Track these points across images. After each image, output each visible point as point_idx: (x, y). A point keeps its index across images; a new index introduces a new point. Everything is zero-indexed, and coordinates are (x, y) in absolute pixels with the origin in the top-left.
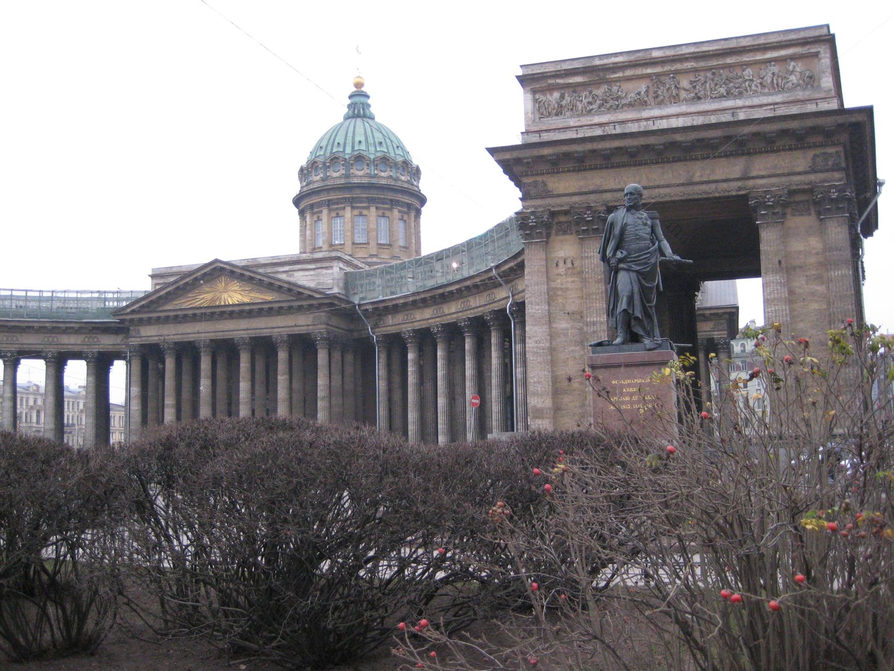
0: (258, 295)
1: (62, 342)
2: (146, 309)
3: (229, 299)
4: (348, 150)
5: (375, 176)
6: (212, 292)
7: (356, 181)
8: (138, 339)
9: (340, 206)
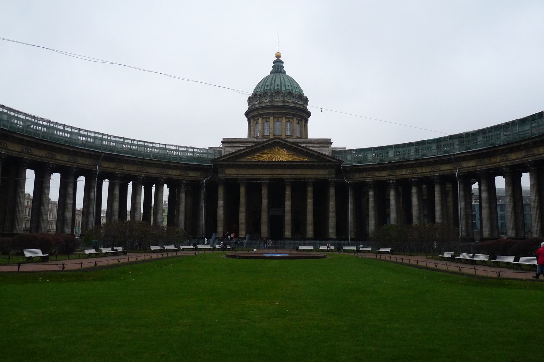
0: (297, 158)
1: (169, 173)
3: (280, 158)
4: (283, 89)
5: (296, 103)
6: (271, 154)
7: (288, 104)
8: (224, 175)
9: (279, 116)
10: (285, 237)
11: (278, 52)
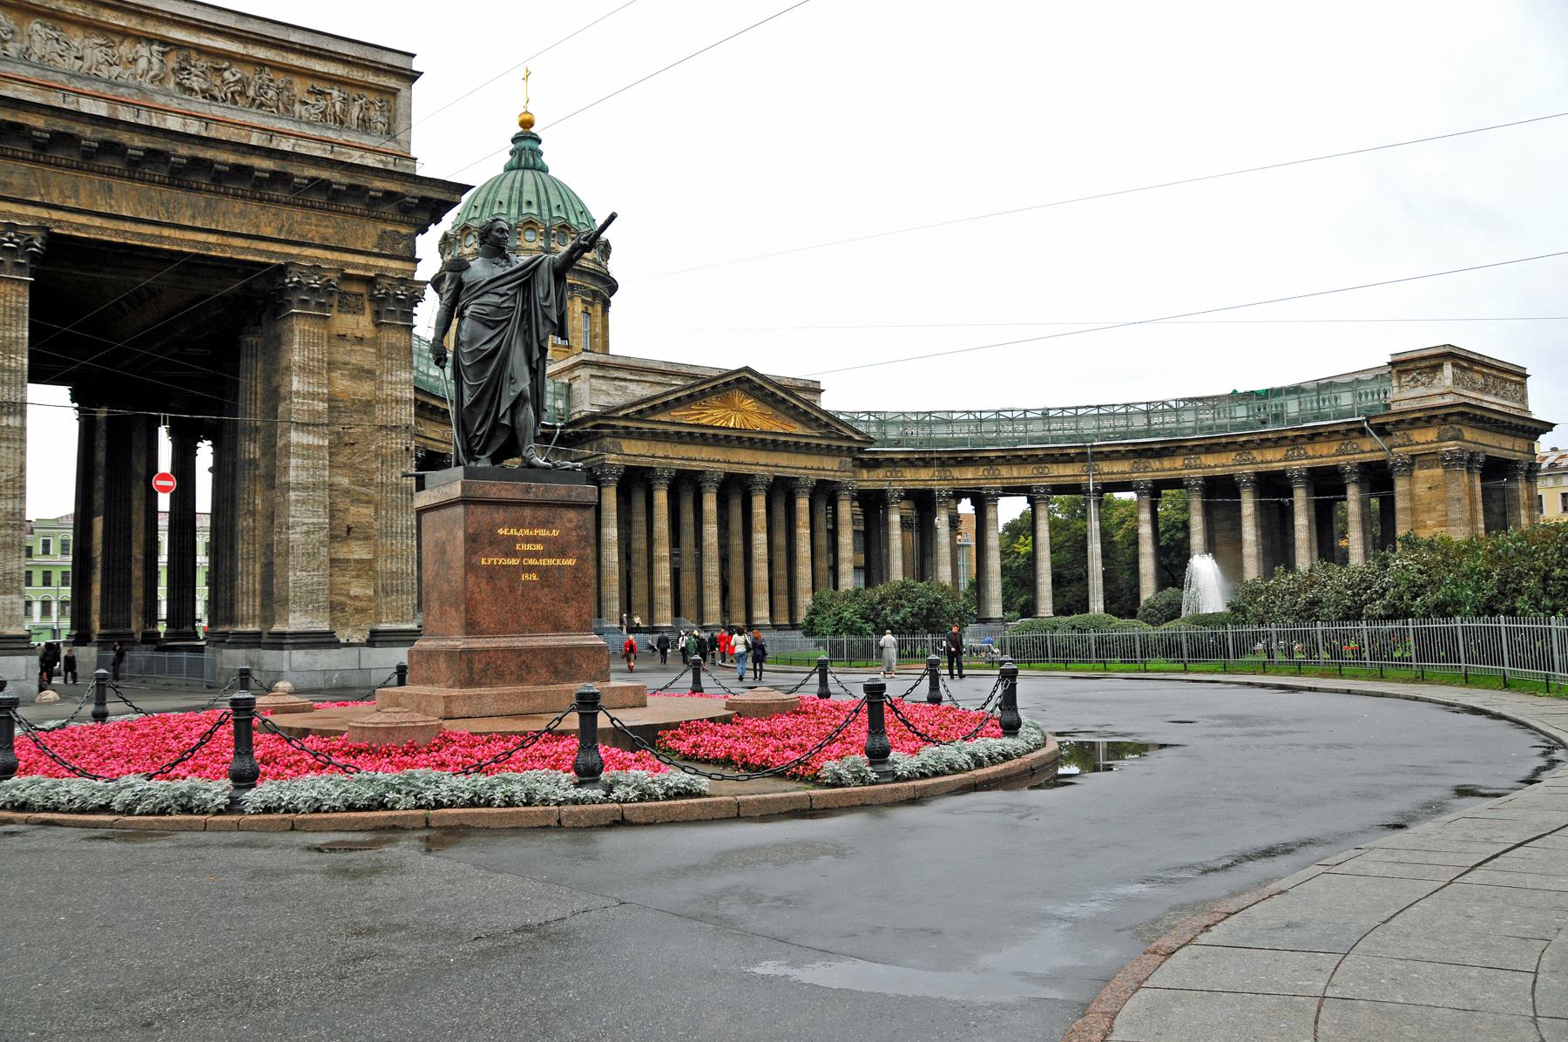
2: (638, 416)
4: (573, 221)
5: (600, 265)
8: (620, 457)
10: (758, 622)
11: (526, 112)
